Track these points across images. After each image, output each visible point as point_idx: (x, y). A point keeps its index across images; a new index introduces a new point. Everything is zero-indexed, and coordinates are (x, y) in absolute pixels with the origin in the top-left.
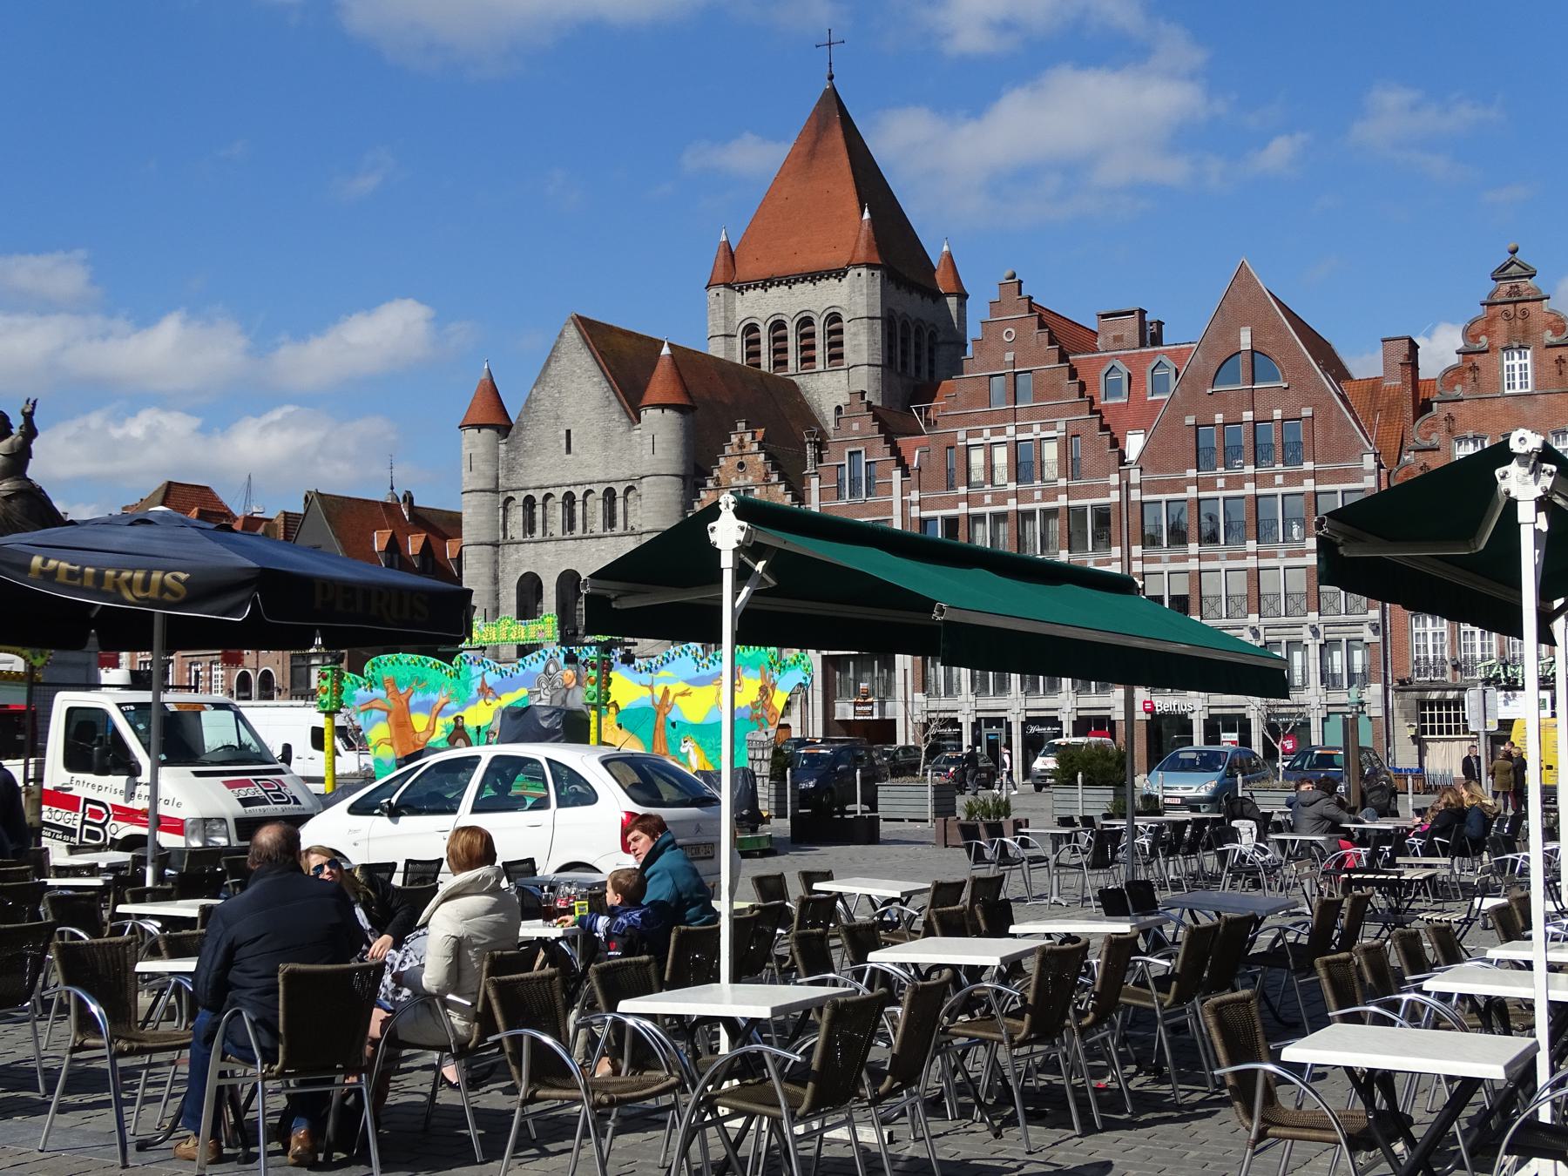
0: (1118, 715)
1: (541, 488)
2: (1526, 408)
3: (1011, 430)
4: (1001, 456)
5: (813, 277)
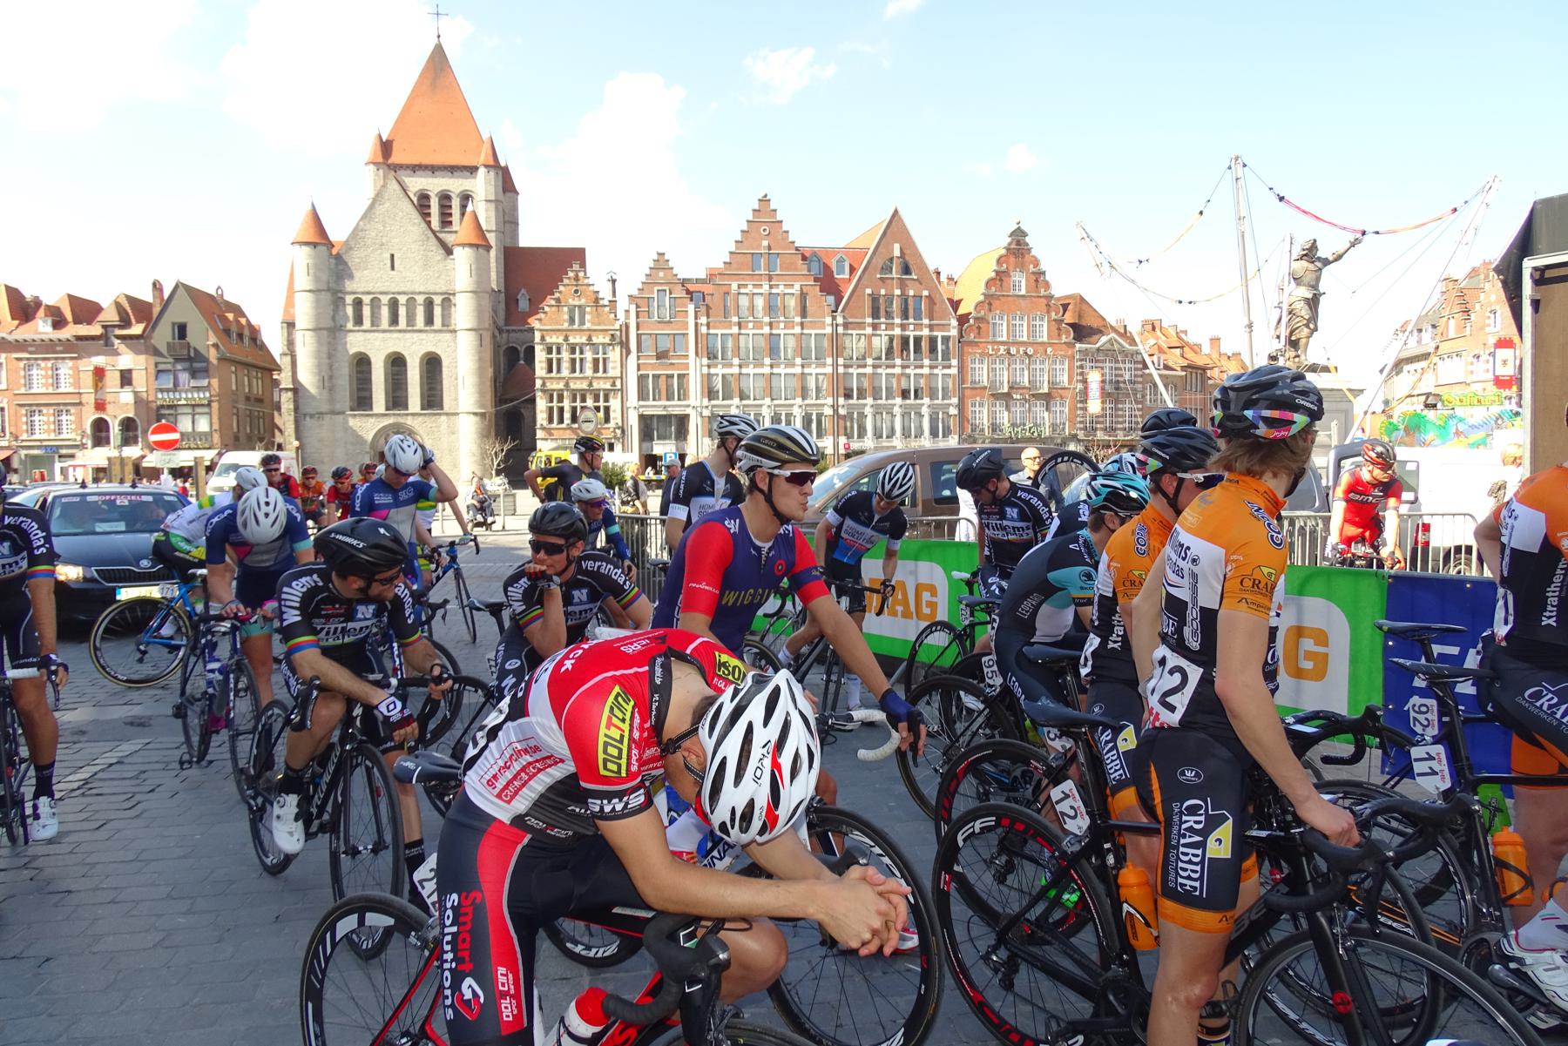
0: (829, 451)
2: (1023, 303)
3: (766, 287)
4: (760, 302)
5: (453, 170)
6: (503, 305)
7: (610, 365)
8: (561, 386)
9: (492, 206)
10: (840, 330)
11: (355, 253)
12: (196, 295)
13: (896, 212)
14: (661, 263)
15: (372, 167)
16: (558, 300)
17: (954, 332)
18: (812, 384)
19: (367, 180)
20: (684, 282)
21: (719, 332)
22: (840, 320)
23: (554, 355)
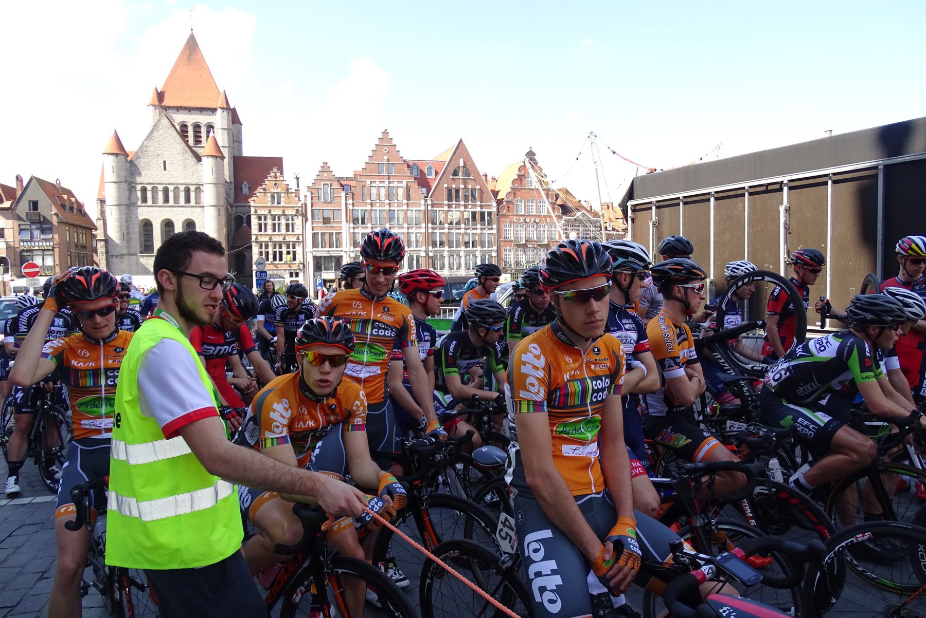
1: (150, 184)
3: (387, 183)
4: (383, 192)
5: (201, 110)
6: (233, 191)
7: (296, 227)
8: (267, 239)
9: (226, 132)
10: (430, 208)
11: (141, 160)
12: (42, 184)
13: (461, 141)
14: (325, 168)
15: (152, 107)
16: (265, 189)
17: (494, 210)
18: (413, 238)
19: (150, 115)
20: (339, 180)
21: (360, 208)
22: (429, 202)
23: (263, 221)
